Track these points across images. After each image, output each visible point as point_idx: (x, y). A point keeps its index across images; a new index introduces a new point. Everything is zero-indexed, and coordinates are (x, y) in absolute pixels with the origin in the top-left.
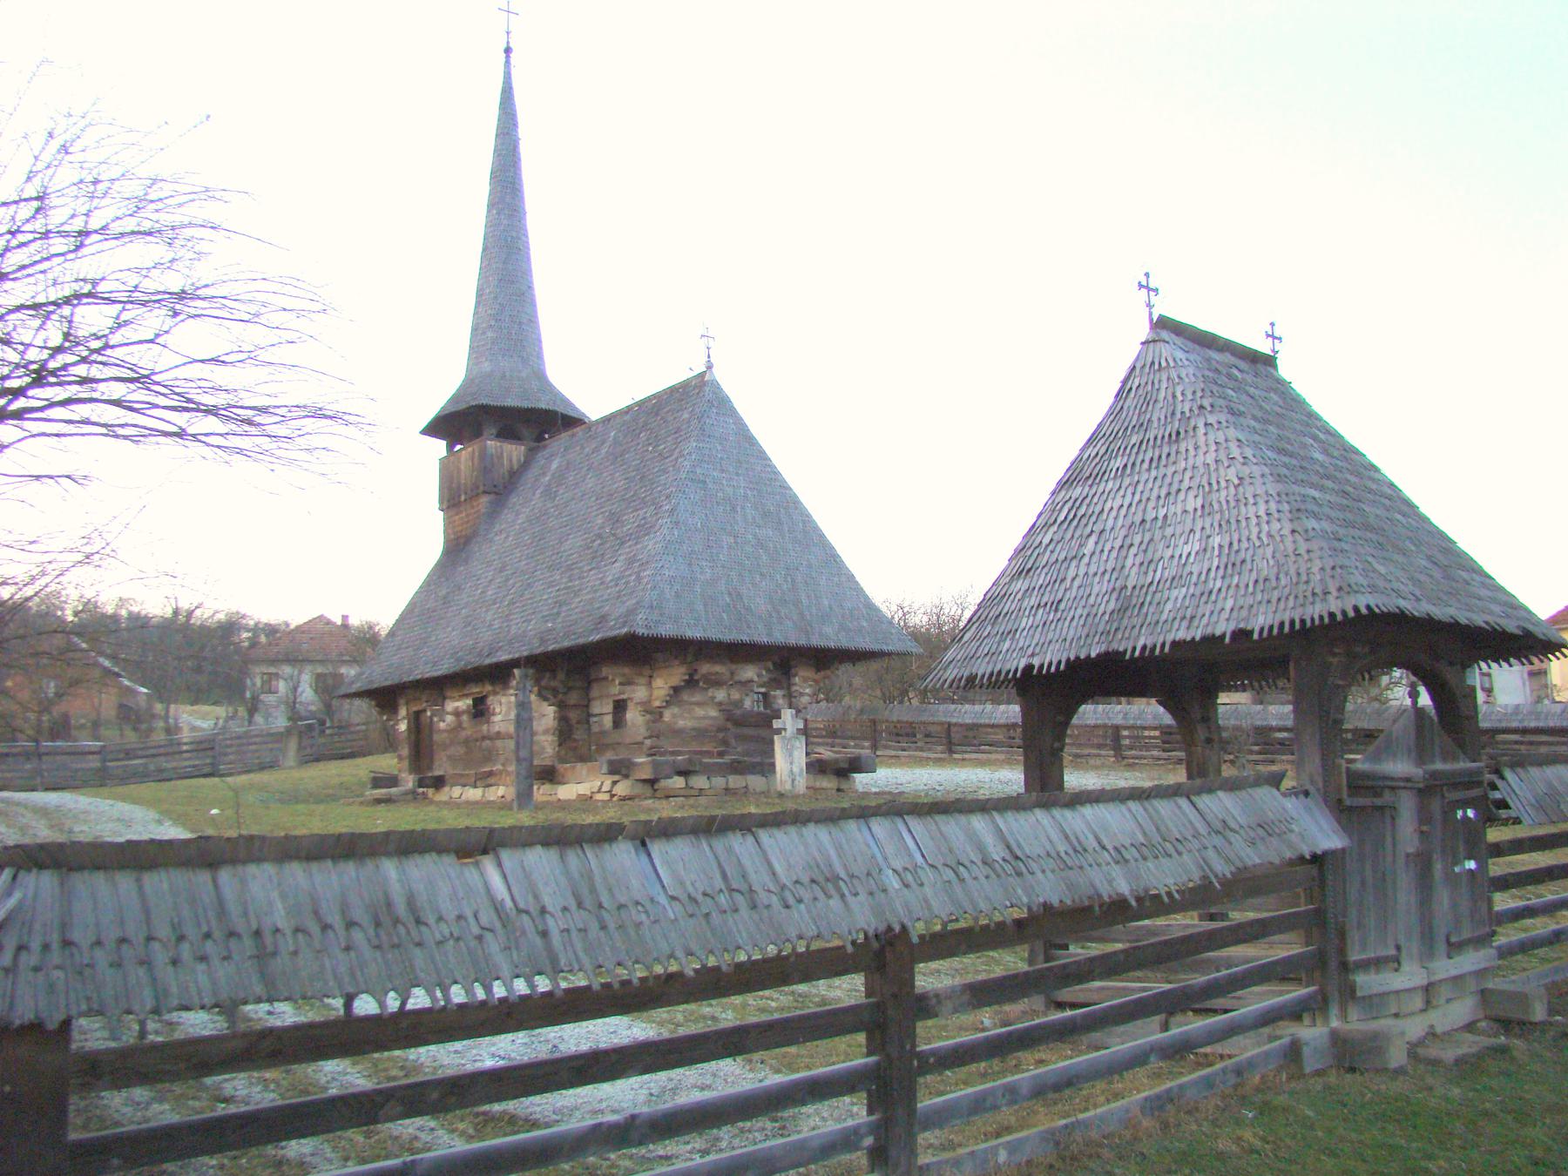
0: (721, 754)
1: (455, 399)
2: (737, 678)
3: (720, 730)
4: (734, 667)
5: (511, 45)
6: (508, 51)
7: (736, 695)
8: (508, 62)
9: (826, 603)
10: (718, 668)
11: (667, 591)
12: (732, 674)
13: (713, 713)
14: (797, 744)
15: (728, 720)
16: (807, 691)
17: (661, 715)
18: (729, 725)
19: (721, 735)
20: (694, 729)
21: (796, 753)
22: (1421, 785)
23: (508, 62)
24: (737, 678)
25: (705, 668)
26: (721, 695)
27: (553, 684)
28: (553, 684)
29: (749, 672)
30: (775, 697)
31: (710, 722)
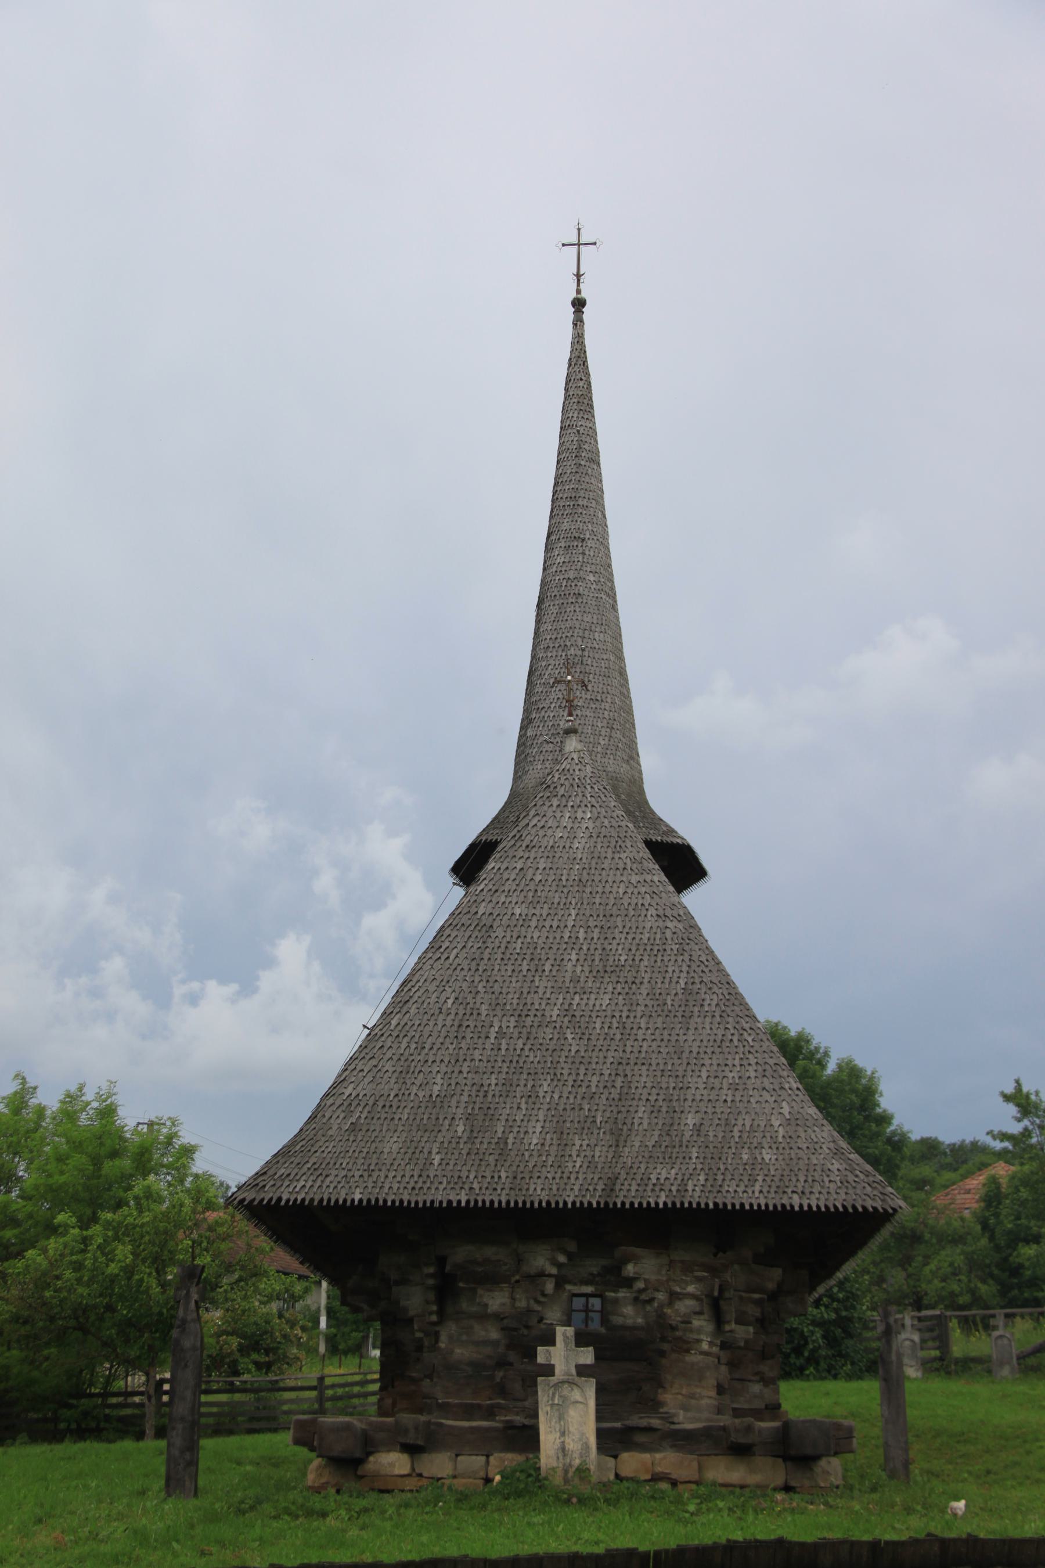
0: (490, 1413)
3: (502, 1363)
5: (583, 295)
6: (579, 304)
7: (522, 1304)
8: (578, 322)
9: (691, 1120)
10: (490, 1252)
11: (335, 1124)
12: (520, 1261)
13: (494, 1335)
14: (576, 1395)
15: (509, 1347)
16: (691, 1289)
17: (437, 1335)
19: (499, 1374)
21: (573, 1415)
23: (578, 322)
25: (461, 1254)
26: (496, 1300)
30: (616, 1301)
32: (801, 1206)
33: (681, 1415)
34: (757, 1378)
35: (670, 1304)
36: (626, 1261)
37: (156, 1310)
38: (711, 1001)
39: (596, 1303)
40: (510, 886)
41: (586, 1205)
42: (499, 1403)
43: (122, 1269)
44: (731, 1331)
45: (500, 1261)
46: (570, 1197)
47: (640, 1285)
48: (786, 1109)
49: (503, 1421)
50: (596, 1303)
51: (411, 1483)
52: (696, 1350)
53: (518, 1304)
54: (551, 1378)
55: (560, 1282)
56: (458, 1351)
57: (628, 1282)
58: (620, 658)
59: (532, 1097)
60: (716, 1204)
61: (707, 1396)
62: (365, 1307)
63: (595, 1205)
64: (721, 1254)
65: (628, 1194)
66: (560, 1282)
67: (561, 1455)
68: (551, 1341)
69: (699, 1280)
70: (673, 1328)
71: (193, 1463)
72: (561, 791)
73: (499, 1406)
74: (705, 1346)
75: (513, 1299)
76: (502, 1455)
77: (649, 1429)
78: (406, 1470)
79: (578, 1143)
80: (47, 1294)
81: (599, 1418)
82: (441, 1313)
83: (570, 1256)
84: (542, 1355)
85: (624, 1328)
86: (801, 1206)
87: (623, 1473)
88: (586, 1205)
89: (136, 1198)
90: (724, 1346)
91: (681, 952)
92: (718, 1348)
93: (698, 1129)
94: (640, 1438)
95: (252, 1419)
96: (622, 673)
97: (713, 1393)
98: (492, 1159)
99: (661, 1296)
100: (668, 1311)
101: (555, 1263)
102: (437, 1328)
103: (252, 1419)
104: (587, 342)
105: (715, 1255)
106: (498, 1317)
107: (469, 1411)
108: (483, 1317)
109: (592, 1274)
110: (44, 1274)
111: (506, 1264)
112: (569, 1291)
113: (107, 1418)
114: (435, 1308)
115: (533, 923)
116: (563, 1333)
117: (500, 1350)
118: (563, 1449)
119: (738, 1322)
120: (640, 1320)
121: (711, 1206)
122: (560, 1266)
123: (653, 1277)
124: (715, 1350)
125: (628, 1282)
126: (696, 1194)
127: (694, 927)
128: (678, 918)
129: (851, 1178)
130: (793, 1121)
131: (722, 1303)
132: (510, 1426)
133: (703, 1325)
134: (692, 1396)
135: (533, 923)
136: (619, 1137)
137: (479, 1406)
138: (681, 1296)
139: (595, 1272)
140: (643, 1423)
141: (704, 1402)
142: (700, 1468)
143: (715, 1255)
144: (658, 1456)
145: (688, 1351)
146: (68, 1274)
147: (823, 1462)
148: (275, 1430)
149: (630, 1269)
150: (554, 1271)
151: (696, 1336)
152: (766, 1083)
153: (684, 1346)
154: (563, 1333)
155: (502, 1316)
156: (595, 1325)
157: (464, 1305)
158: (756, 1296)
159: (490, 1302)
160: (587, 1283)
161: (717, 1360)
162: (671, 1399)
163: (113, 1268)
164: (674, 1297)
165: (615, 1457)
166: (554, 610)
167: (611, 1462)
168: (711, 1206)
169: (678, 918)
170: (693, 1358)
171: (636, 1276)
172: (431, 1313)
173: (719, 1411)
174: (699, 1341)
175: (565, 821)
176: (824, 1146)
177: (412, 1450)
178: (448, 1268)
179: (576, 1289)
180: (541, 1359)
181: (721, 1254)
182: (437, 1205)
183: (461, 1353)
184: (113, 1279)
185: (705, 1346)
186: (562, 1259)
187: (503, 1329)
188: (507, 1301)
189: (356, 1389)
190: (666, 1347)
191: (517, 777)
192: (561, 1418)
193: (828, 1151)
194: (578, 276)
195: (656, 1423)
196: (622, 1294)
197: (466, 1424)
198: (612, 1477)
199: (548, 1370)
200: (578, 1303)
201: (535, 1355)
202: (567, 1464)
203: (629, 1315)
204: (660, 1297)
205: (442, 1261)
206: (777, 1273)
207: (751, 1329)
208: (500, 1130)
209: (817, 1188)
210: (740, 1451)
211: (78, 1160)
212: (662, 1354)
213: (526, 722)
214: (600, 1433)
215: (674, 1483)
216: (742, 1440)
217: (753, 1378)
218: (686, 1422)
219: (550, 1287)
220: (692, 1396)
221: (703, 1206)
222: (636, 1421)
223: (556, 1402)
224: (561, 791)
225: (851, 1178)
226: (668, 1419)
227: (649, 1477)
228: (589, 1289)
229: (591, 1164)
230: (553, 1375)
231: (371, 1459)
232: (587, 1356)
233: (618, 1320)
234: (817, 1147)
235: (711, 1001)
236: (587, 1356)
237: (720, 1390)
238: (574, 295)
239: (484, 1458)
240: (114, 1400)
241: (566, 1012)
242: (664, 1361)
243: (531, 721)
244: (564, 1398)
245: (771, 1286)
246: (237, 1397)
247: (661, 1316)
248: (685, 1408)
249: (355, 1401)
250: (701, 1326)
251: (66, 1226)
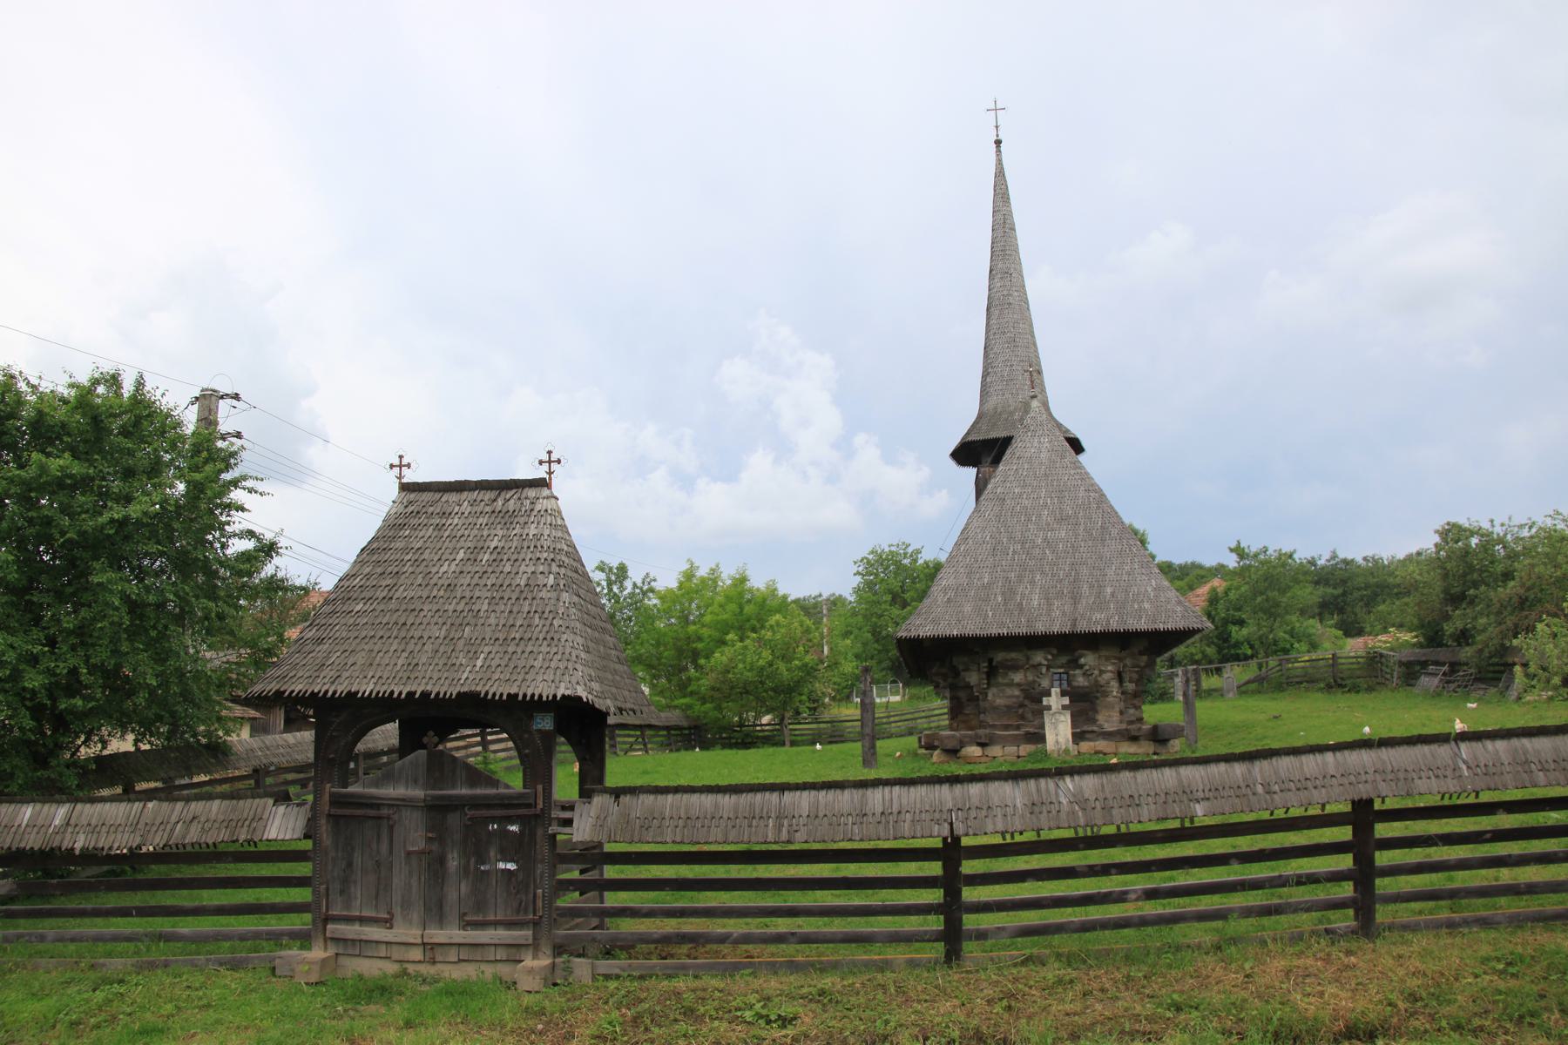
0: (1018, 728)
1: (963, 439)
2: (1031, 662)
3: (1022, 705)
4: (1029, 653)
6: (998, 143)
7: (1030, 678)
8: (998, 151)
9: (1109, 590)
10: (1013, 655)
11: (940, 599)
12: (1028, 659)
13: (1017, 693)
14: (1062, 718)
15: (1025, 698)
16: (1110, 668)
17: (986, 694)
18: (1026, 702)
19: (1021, 711)
20: (1006, 706)
22: (423, 804)
23: (998, 151)
24: (1031, 662)
25: (1000, 657)
26: (1018, 677)
27: (944, 670)
28: (944, 670)
29: (1039, 657)
30: (1074, 675)
31: (1014, 700)
33: (1106, 725)
35: (1100, 675)
36: (1080, 657)
37: (786, 683)
38: (1114, 532)
39: (1065, 676)
40: (1011, 478)
43: (767, 663)
46: (1056, 629)
47: (1087, 667)
48: (1154, 583)
50: (1065, 676)
51: (984, 759)
55: (1048, 667)
57: (1081, 667)
58: (1033, 336)
59: (1032, 582)
61: (1116, 716)
62: (941, 681)
65: (1083, 627)
66: (1048, 667)
68: (1049, 695)
69: (1114, 664)
70: (1102, 686)
71: (874, 754)
72: (1032, 428)
73: (1022, 725)
74: (1115, 693)
75: (1026, 677)
77: (1093, 732)
78: (980, 754)
80: (730, 676)
81: (1072, 728)
82: (988, 684)
83: (1053, 655)
84: (1045, 701)
85: (1079, 687)
87: (1082, 751)
89: (772, 626)
90: (1123, 693)
91: (1098, 508)
93: (1113, 595)
94: (1088, 736)
95: (831, 736)
96: (1035, 344)
98: (1016, 613)
99: (1096, 672)
100: (1099, 679)
101: (1046, 659)
103: (831, 736)
104: (1004, 163)
106: (1019, 685)
107: (1007, 727)
108: (1011, 684)
110: (726, 666)
113: (758, 737)
115: (1025, 496)
116: (1055, 691)
118: (1057, 742)
119: (1130, 682)
120: (1086, 684)
122: (1048, 660)
123: (1092, 664)
125: (1081, 667)
126: (1115, 625)
127: (1104, 495)
128: (1095, 491)
129: (1186, 614)
130: (1157, 589)
132: (1028, 733)
133: (1114, 684)
134: (1110, 716)
135: (1025, 496)
136: (1075, 599)
140: (1090, 729)
141: (1115, 719)
142: (1116, 748)
144: (1097, 743)
146: (741, 666)
147: (1172, 742)
148: (843, 742)
149: (1082, 661)
150: (1046, 663)
152: (1144, 571)
153: (1106, 694)
154: (1055, 691)
156: (1065, 686)
157: (1000, 680)
160: (1061, 667)
162: (1101, 718)
163: (761, 662)
164: (1102, 672)
166: (997, 312)
169: (1095, 491)
170: (1110, 699)
173: (1121, 722)
175: (1036, 444)
177: (983, 745)
178: (994, 664)
179: (1056, 671)
180: (1045, 703)
183: (999, 702)
184: (762, 668)
185: (1115, 693)
186: (1050, 657)
189: (884, 720)
190: (1099, 695)
191: (982, 403)
192: (1056, 728)
194: (997, 127)
195: (1095, 729)
196: (1078, 672)
199: (1049, 708)
200: (1056, 677)
201: (1041, 702)
203: (1081, 681)
205: (990, 661)
206: (1145, 658)
209: (1171, 620)
210: (1134, 739)
211: (733, 607)
212: (1097, 698)
213: (985, 375)
214: (1074, 735)
215: (1105, 754)
216: (1137, 734)
218: (1108, 727)
219: (1044, 670)
220: (1110, 716)
222: (1086, 728)
224: (1032, 428)
225: (1186, 614)
226: (1101, 726)
228: (1062, 670)
229: (1064, 613)
231: (963, 750)
232: (1066, 701)
233: (1075, 684)
235: (1114, 532)
236: (1066, 701)
237: (1121, 713)
238: (995, 138)
239: (1016, 748)
240: (758, 728)
241: (1045, 540)
242: (1098, 702)
243: (988, 374)
244: (1056, 720)
245: (1142, 664)
246: (822, 725)
247: (1096, 681)
248: (1106, 721)
249: (885, 726)
251: (732, 641)
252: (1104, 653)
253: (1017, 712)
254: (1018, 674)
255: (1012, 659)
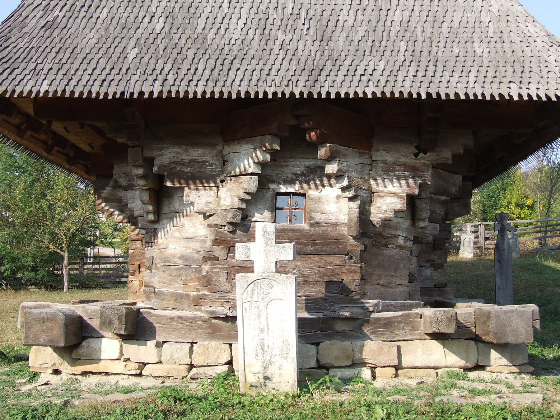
0: (197, 302)
3: (209, 258)
4: (227, 150)
10: (196, 153)
19: (206, 268)
20: (183, 258)
32: (520, 96)
34: (429, 264)
41: (288, 96)
42: (205, 295)
44: (424, 228)
45: (206, 162)
49: (207, 312)
52: (393, 244)
53: (223, 202)
54: (249, 275)
56: (171, 246)
60: (429, 94)
63: (298, 96)
64: (421, 155)
67: (260, 352)
74: (401, 241)
76: (206, 343)
79: (281, 37)
83: (273, 153)
86: (520, 96)
87: (324, 361)
88: (288, 96)
90: (417, 240)
92: (411, 243)
94: (340, 326)
97: (406, 282)
102: (156, 226)
105: (416, 155)
109: (296, 174)
111: (211, 165)
112: (273, 190)
114: (150, 208)
117: (207, 246)
121: (424, 96)
124: (409, 244)
131: (418, 202)
134: (389, 285)
137: (188, 296)
138: (382, 194)
139: (299, 172)
143: (416, 155)
145: (386, 245)
151: (394, 232)
155: (208, 214)
158: (443, 198)
159: (197, 201)
161: (410, 253)
165: (317, 344)
167: (313, 349)
168: (424, 96)
170: (390, 251)
171: (340, 173)
172: (148, 213)
174: (396, 236)
176: (537, 39)
181: (421, 155)
182: (127, 96)
185: (401, 241)
187: (209, 226)
188: (214, 200)
193: (542, 44)
197: (174, 313)
198: (313, 364)
202: (267, 361)
204: (363, 194)
205: (149, 162)
206: (458, 179)
207: (438, 226)
208: (201, 26)
217: (426, 265)
221: (415, 96)
223: (255, 299)
227: (350, 363)
230: (253, 271)
231: (84, 343)
234: (531, 40)
237: (412, 278)
250: (398, 223)
252: (381, 155)
253: (199, 270)
254: (202, 192)
255: (192, 162)
